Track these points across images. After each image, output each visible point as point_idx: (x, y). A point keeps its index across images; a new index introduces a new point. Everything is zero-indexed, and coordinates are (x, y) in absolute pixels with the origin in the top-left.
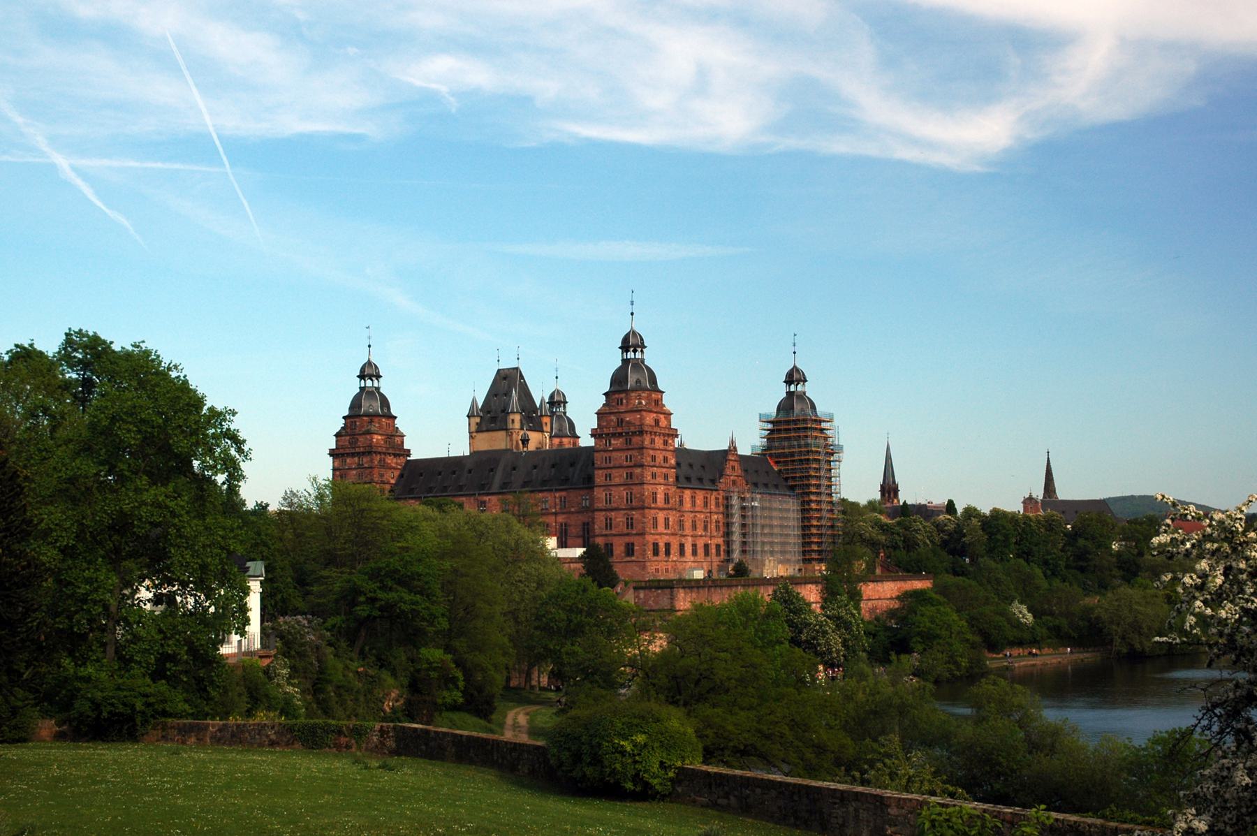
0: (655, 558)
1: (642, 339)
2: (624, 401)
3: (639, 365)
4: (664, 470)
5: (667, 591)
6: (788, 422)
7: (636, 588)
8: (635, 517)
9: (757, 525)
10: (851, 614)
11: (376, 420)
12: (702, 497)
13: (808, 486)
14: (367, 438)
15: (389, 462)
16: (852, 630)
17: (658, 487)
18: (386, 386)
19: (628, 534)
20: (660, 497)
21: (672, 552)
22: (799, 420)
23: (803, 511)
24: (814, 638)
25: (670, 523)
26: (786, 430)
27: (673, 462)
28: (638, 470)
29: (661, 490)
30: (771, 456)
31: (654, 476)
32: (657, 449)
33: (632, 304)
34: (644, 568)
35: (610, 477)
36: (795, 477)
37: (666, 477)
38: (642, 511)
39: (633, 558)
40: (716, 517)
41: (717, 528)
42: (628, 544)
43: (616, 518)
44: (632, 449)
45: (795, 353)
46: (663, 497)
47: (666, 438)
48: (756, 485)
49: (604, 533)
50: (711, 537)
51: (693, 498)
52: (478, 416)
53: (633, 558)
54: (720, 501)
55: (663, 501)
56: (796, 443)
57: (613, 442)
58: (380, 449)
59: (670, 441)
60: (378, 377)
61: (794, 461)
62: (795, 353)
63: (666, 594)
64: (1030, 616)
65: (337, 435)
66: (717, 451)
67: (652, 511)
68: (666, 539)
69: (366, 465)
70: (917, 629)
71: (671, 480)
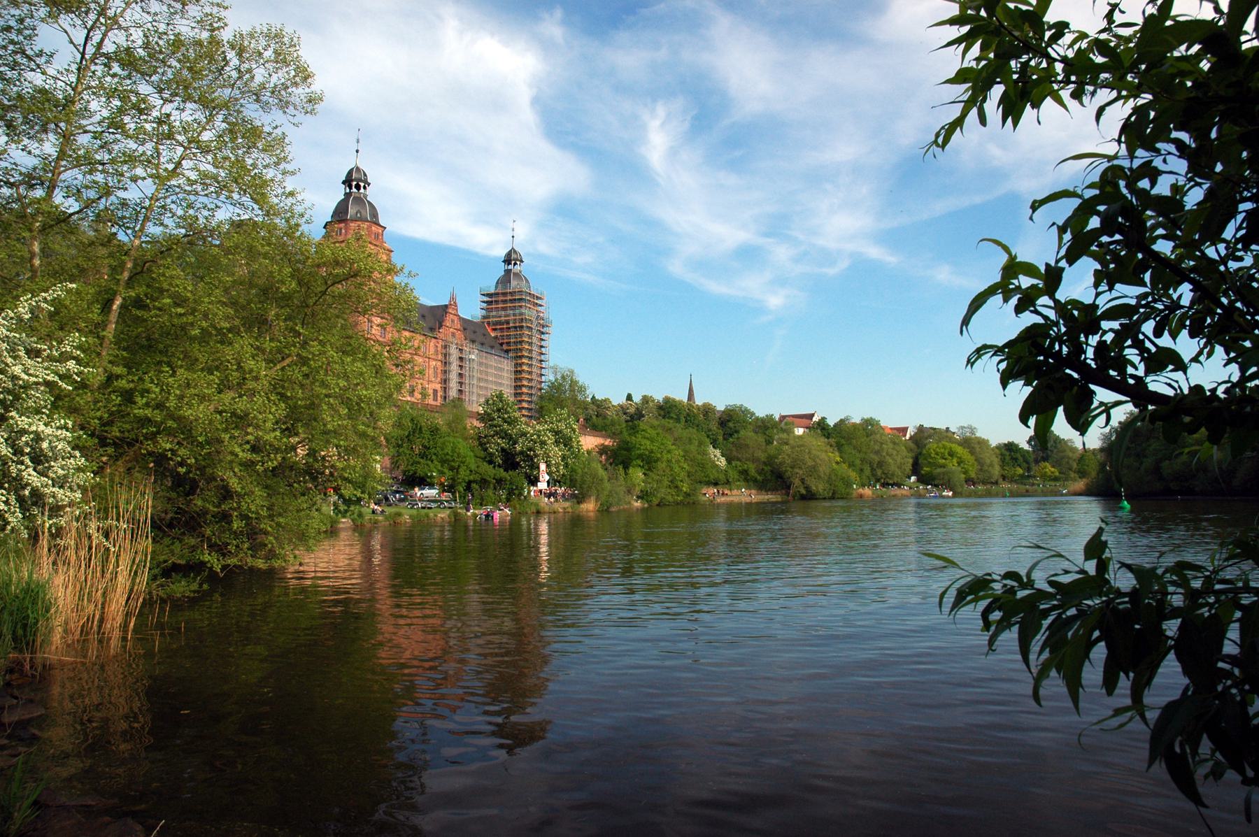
1: (365, 175)
2: (343, 231)
3: (360, 201)
6: (505, 294)
9: (473, 392)
10: (571, 428)
13: (521, 350)
16: (572, 447)
22: (515, 292)
23: (516, 372)
24: (530, 449)
26: (502, 301)
30: (489, 323)
33: (358, 142)
36: (510, 342)
40: (434, 363)
41: (436, 373)
48: (473, 341)
50: (429, 382)
54: (439, 349)
56: (511, 312)
61: (509, 328)
64: (723, 460)
66: (438, 306)
70: (638, 452)
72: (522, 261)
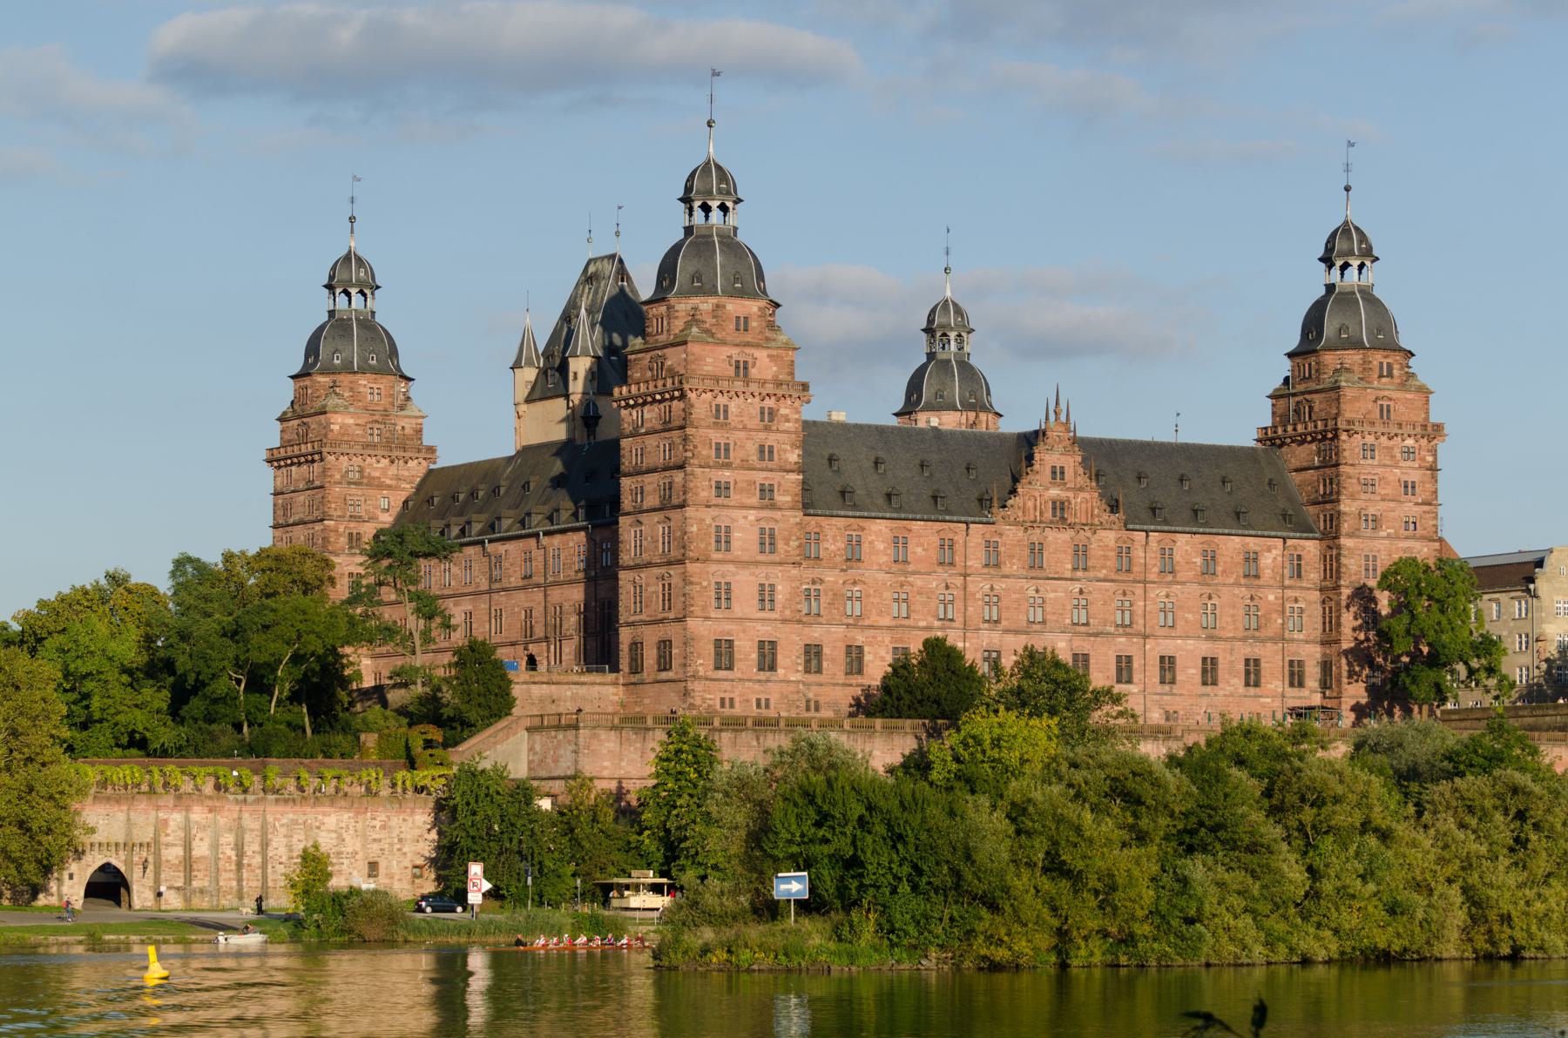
0: (722, 674)
4: (760, 477)
5: (571, 734)
7: (528, 729)
8: (674, 581)
11: (345, 379)
12: (935, 540)
14: (320, 424)
15: (377, 474)
17: (737, 514)
18: (387, 310)
19: (661, 621)
20: (744, 536)
21: (781, 659)
25: (779, 597)
27: (793, 457)
28: (678, 477)
29: (745, 526)
31: (722, 489)
32: (735, 429)
34: (686, 693)
35: (642, 493)
37: (766, 492)
38: (679, 568)
39: (670, 675)
42: (664, 642)
43: (648, 585)
44: (670, 430)
45: (1347, 189)
46: (754, 536)
47: (769, 403)
49: (632, 619)
51: (899, 542)
52: (530, 363)
53: (670, 675)
55: (756, 547)
57: (646, 416)
58: (344, 448)
59: (783, 411)
60: (369, 287)
62: (1347, 189)
63: (569, 742)
65: (282, 419)
67: (713, 568)
68: (765, 631)
69: (317, 483)
71: (788, 498)
72: (1368, 253)
